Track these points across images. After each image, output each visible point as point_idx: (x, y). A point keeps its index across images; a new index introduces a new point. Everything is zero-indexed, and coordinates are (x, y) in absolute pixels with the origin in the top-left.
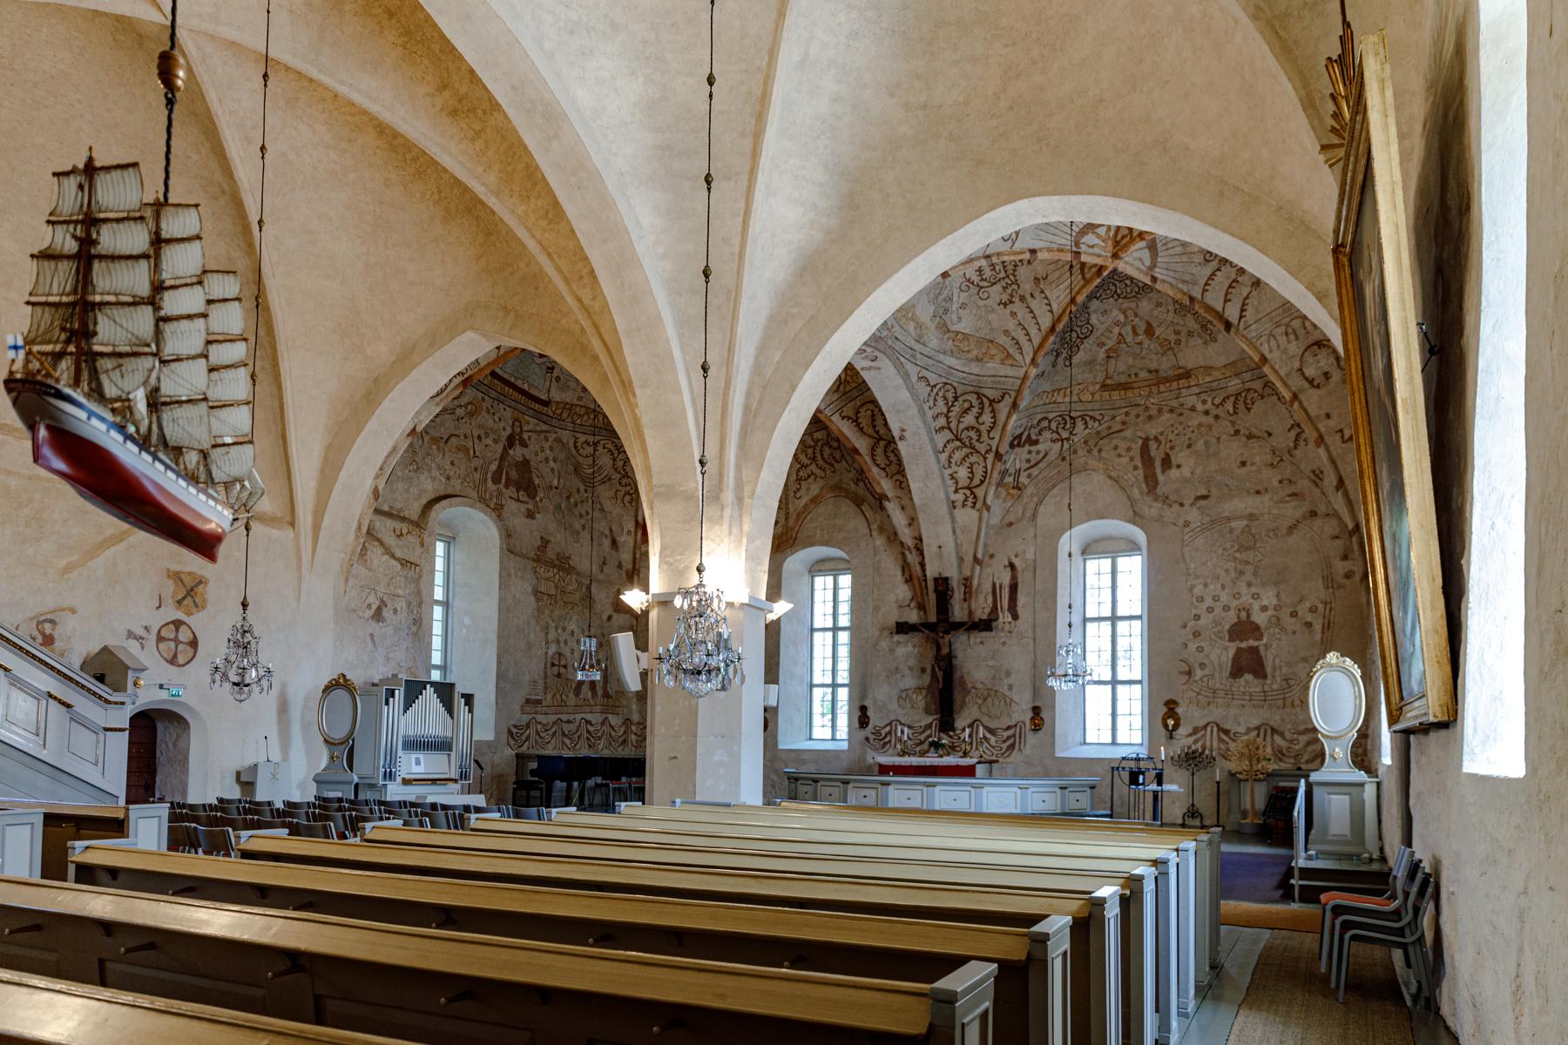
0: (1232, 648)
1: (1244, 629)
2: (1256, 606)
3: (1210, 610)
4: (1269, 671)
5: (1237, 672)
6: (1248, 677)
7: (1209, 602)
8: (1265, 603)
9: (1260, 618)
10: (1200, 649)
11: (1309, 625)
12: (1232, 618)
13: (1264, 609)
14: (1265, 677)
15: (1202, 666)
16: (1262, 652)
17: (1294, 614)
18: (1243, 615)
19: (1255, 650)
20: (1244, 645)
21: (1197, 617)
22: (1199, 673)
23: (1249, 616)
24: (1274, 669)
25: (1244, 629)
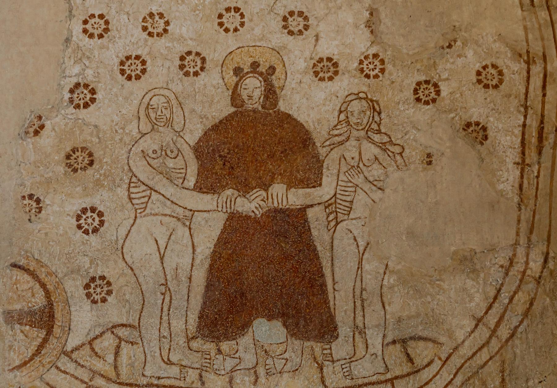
0: (210, 216)
1: (253, 143)
2: (298, 56)
3: (133, 68)
4: (341, 304)
5: (226, 309)
6: (267, 331)
7: (128, 38)
8: (326, 49)
9: (311, 104)
10: (91, 220)
11: (477, 132)
12: (208, 101)
13: (326, 69)
14: (327, 330)
15: (97, 288)
16: (319, 234)
17: (426, 92)
18: (253, 87)
19: (291, 224)
20: (251, 205)
21: (84, 95)
22: (83, 319)
23: (271, 93)
24: (360, 301)
25: (253, 143)
